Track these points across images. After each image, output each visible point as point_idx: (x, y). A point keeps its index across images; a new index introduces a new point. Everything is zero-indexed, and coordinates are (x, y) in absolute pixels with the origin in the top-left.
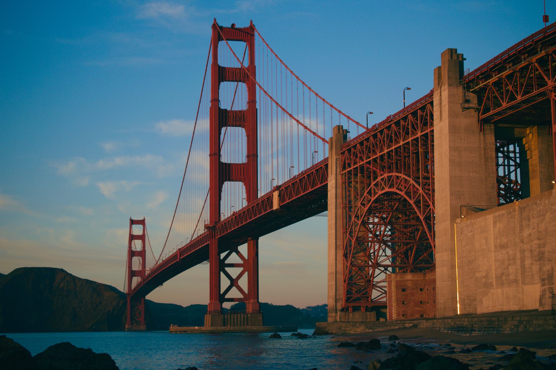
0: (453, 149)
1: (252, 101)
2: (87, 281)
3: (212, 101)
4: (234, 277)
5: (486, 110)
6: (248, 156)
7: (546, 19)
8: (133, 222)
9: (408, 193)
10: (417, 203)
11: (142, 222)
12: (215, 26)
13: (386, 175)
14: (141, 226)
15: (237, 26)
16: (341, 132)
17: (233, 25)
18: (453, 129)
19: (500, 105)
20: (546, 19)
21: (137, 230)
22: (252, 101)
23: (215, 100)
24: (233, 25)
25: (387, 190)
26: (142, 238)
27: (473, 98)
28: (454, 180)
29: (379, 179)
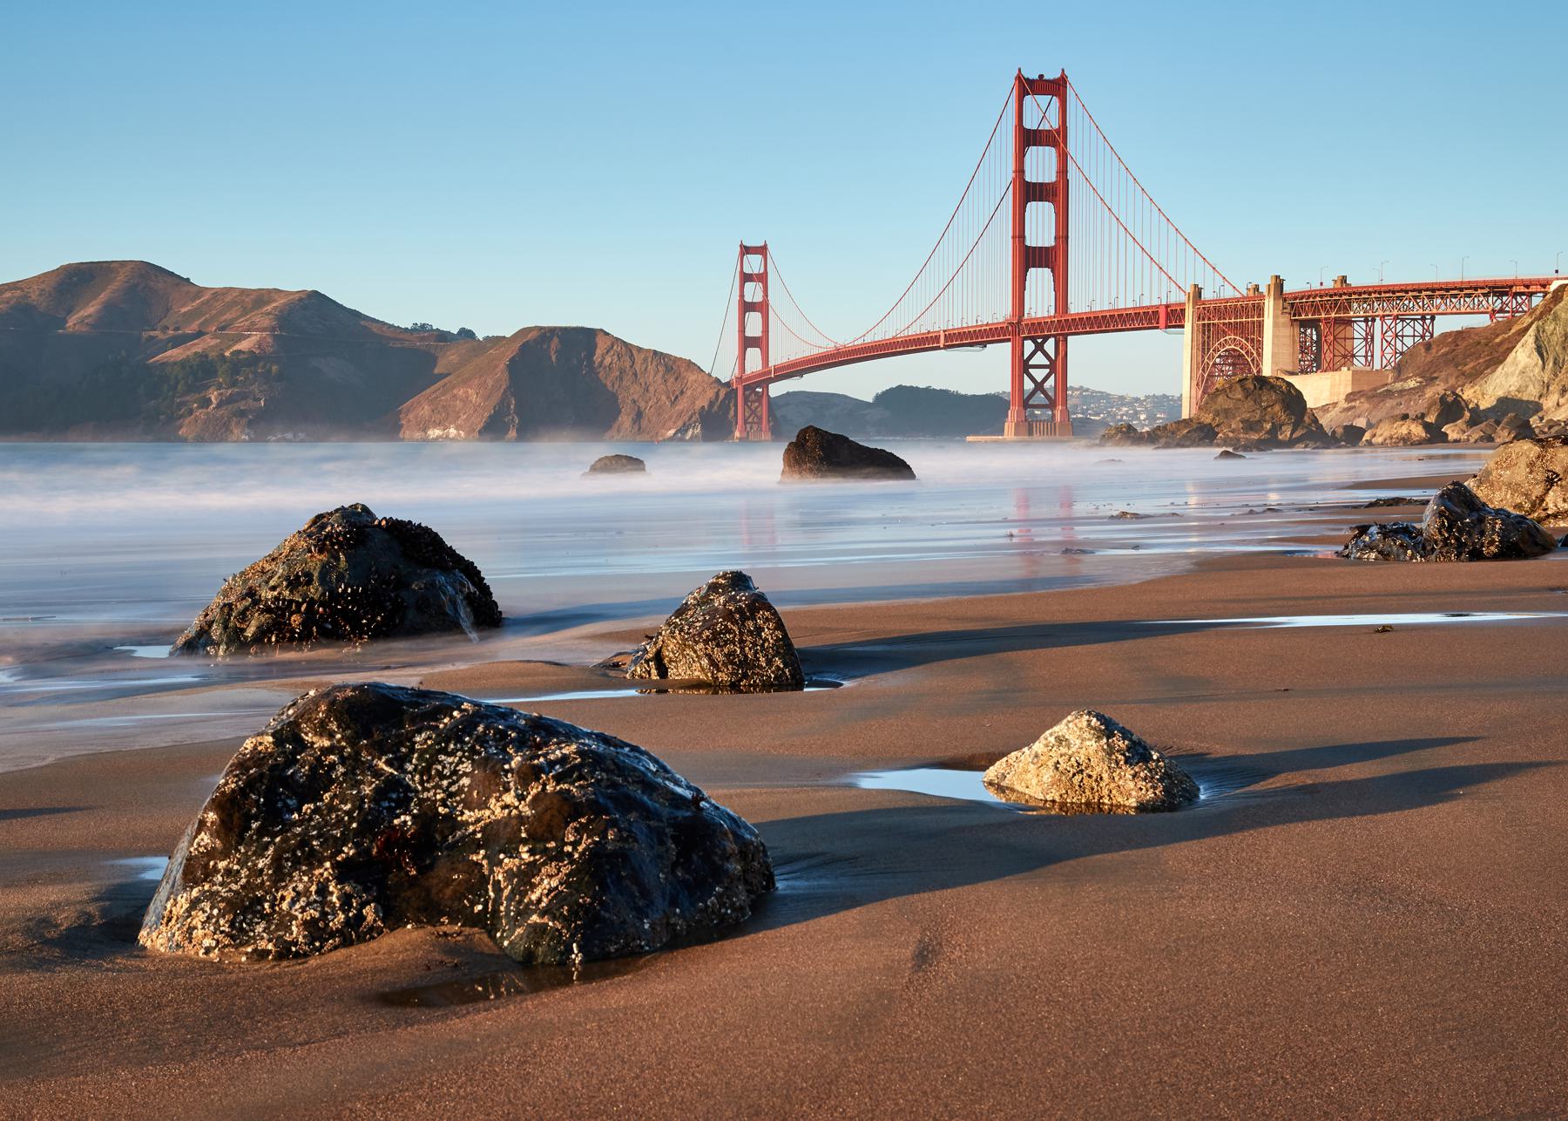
0: (1274, 336)
1: (1063, 171)
2: (655, 352)
3: (1015, 172)
4: (1039, 380)
5: (1295, 315)
6: (1056, 238)
7: (1322, 284)
8: (746, 250)
9: (1247, 353)
10: (1253, 360)
11: (762, 250)
12: (1020, 78)
13: (1233, 337)
14: (759, 257)
15: (1046, 77)
16: (1198, 291)
17: (1041, 76)
18: (1276, 325)
19: (1300, 315)
20: (1322, 284)
21: (754, 264)
22: (1063, 171)
23: (1020, 171)
24: (1041, 76)
25: (1233, 347)
26: (762, 278)
27: (1286, 305)
28: (1274, 355)
29: (1227, 338)
